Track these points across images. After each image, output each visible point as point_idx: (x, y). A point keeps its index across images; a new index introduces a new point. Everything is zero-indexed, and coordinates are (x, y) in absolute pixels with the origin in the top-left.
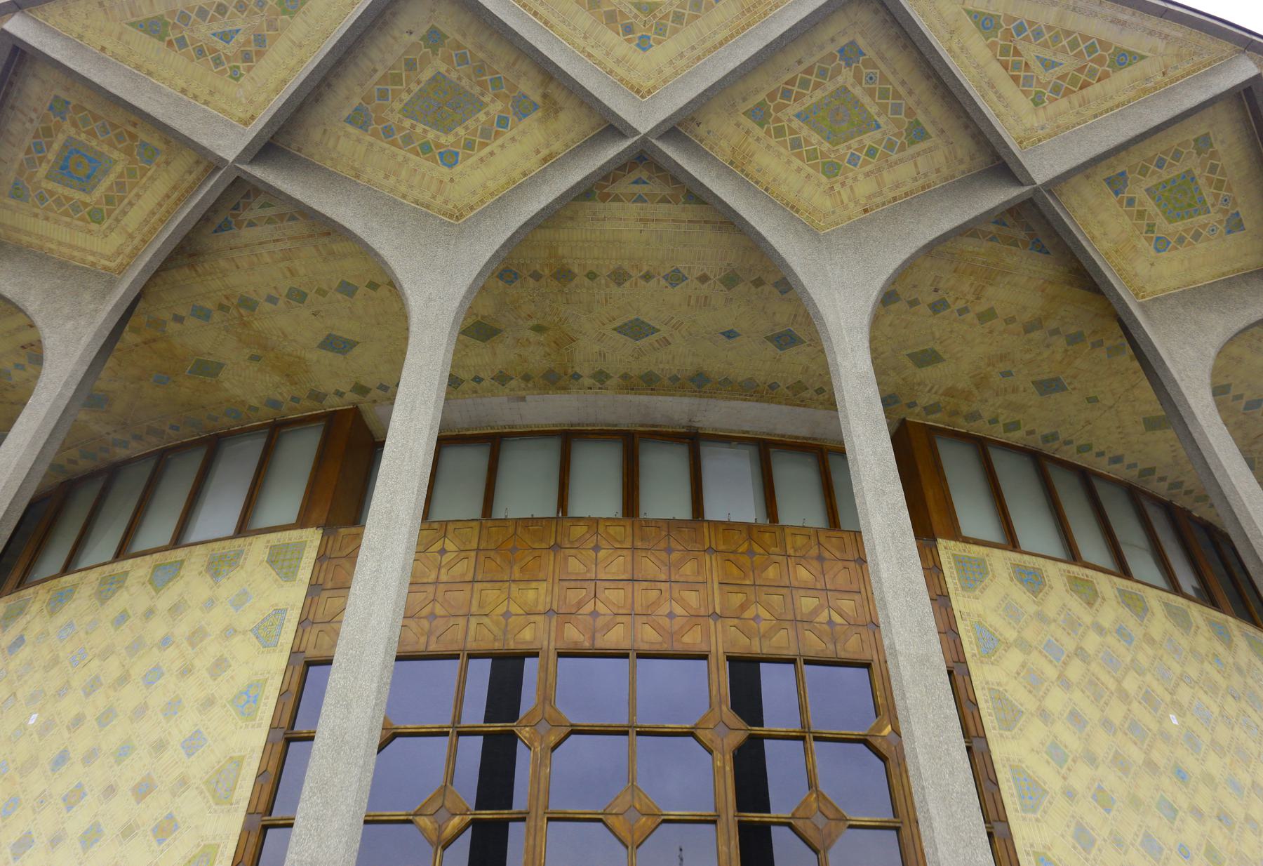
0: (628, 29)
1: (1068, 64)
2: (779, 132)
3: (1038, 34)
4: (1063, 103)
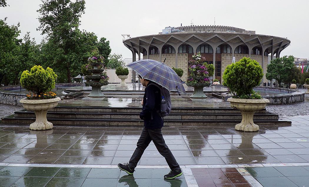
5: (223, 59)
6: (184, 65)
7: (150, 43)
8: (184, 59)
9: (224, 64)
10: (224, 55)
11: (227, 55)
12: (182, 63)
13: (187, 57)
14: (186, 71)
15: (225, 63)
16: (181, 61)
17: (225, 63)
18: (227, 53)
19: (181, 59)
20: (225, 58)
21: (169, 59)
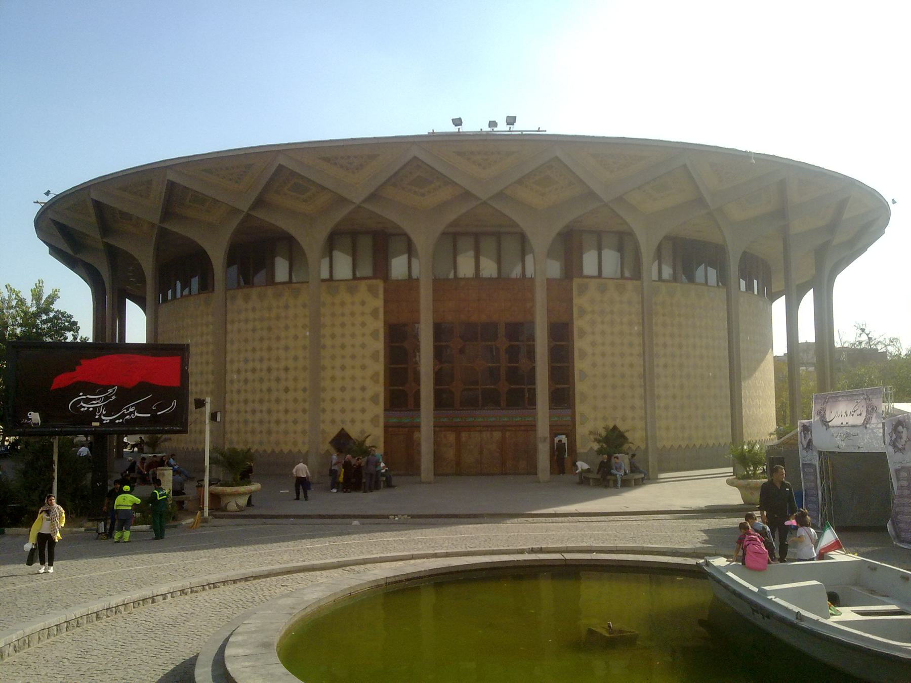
5: (583, 312)
6: (363, 346)
7: (156, 218)
8: (363, 314)
11: (603, 290)
12: (353, 335)
13: (379, 303)
14: (377, 382)
16: (343, 325)
18: (600, 275)
19: (343, 315)
21: (278, 318)
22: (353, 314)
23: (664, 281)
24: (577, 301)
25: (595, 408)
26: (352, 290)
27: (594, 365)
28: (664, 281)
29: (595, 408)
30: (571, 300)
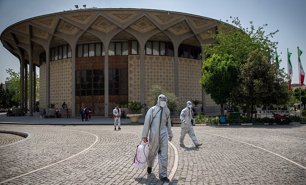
0: (81, 20)
1: (125, 16)
2: (99, 26)
3: (120, 14)
4: (126, 19)
5: (131, 65)
8: (69, 68)
9: (133, 74)
10: (133, 58)
15: (135, 72)
17: (135, 72)
20: (135, 62)
22: (67, 68)
23: (161, 55)
24: (129, 62)
25: (135, 95)
26: (67, 62)
27: (135, 82)
28: (161, 55)
29: (135, 95)
30: (128, 62)
